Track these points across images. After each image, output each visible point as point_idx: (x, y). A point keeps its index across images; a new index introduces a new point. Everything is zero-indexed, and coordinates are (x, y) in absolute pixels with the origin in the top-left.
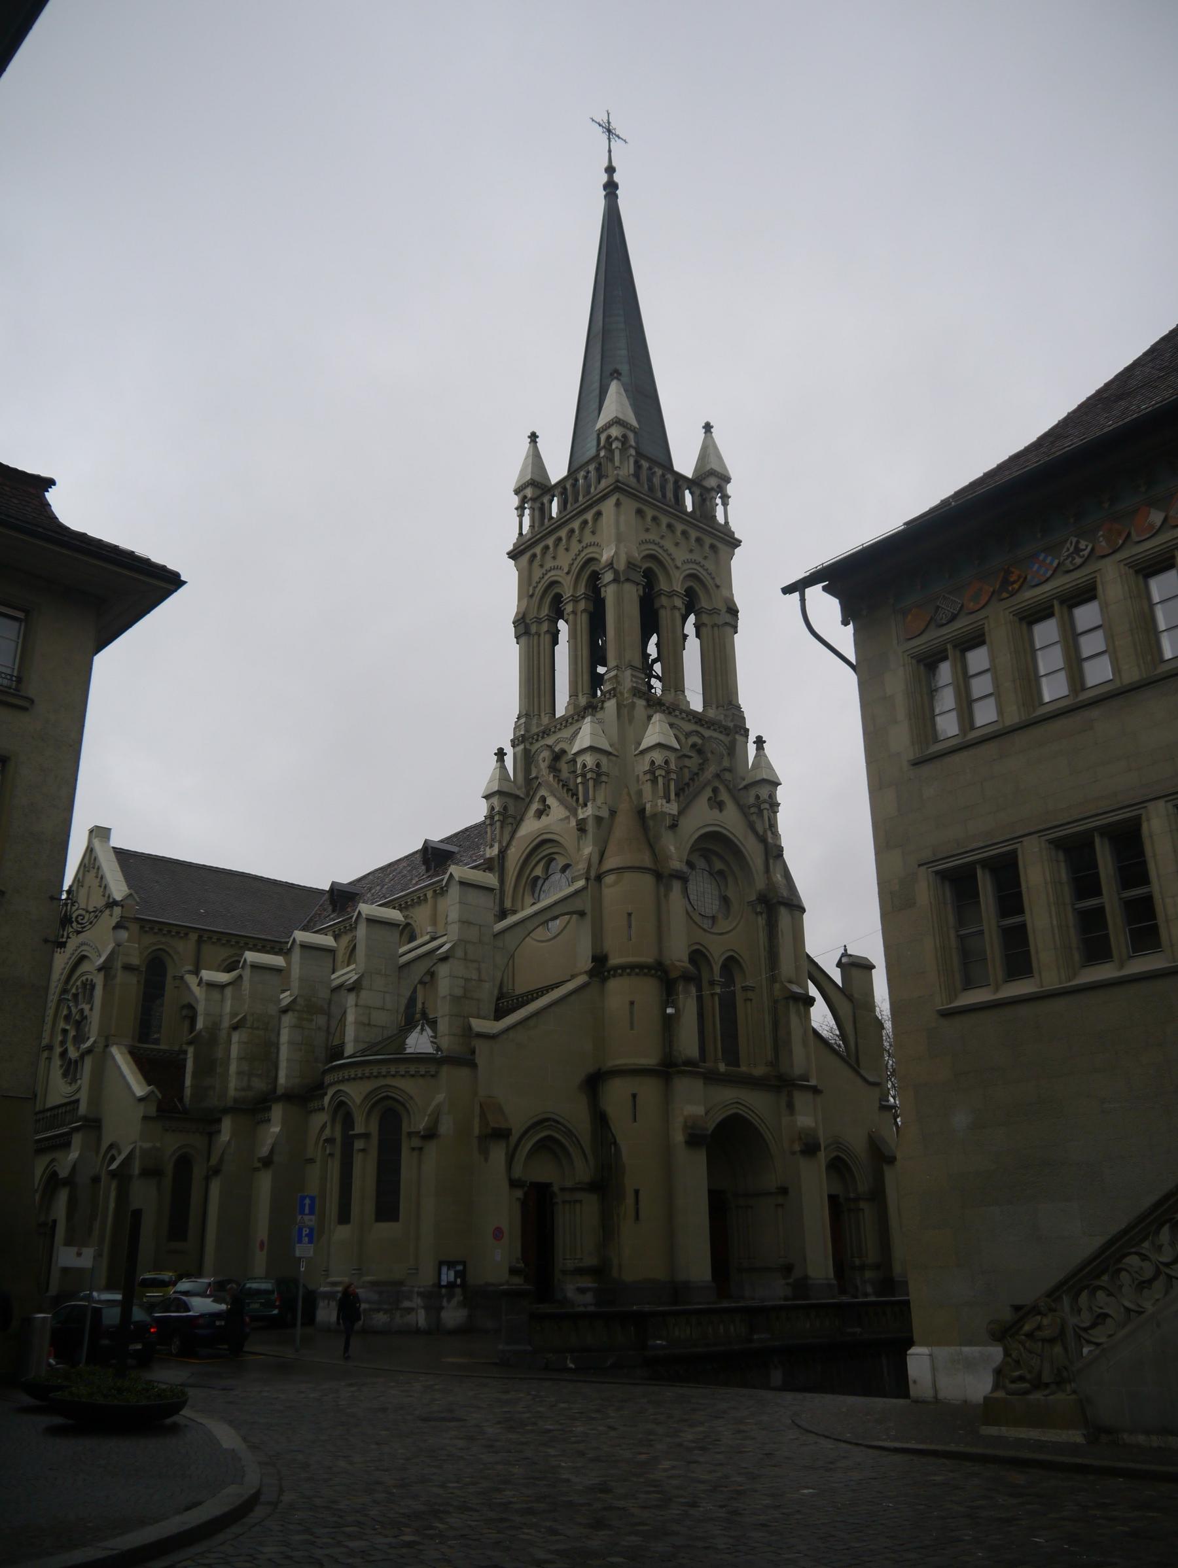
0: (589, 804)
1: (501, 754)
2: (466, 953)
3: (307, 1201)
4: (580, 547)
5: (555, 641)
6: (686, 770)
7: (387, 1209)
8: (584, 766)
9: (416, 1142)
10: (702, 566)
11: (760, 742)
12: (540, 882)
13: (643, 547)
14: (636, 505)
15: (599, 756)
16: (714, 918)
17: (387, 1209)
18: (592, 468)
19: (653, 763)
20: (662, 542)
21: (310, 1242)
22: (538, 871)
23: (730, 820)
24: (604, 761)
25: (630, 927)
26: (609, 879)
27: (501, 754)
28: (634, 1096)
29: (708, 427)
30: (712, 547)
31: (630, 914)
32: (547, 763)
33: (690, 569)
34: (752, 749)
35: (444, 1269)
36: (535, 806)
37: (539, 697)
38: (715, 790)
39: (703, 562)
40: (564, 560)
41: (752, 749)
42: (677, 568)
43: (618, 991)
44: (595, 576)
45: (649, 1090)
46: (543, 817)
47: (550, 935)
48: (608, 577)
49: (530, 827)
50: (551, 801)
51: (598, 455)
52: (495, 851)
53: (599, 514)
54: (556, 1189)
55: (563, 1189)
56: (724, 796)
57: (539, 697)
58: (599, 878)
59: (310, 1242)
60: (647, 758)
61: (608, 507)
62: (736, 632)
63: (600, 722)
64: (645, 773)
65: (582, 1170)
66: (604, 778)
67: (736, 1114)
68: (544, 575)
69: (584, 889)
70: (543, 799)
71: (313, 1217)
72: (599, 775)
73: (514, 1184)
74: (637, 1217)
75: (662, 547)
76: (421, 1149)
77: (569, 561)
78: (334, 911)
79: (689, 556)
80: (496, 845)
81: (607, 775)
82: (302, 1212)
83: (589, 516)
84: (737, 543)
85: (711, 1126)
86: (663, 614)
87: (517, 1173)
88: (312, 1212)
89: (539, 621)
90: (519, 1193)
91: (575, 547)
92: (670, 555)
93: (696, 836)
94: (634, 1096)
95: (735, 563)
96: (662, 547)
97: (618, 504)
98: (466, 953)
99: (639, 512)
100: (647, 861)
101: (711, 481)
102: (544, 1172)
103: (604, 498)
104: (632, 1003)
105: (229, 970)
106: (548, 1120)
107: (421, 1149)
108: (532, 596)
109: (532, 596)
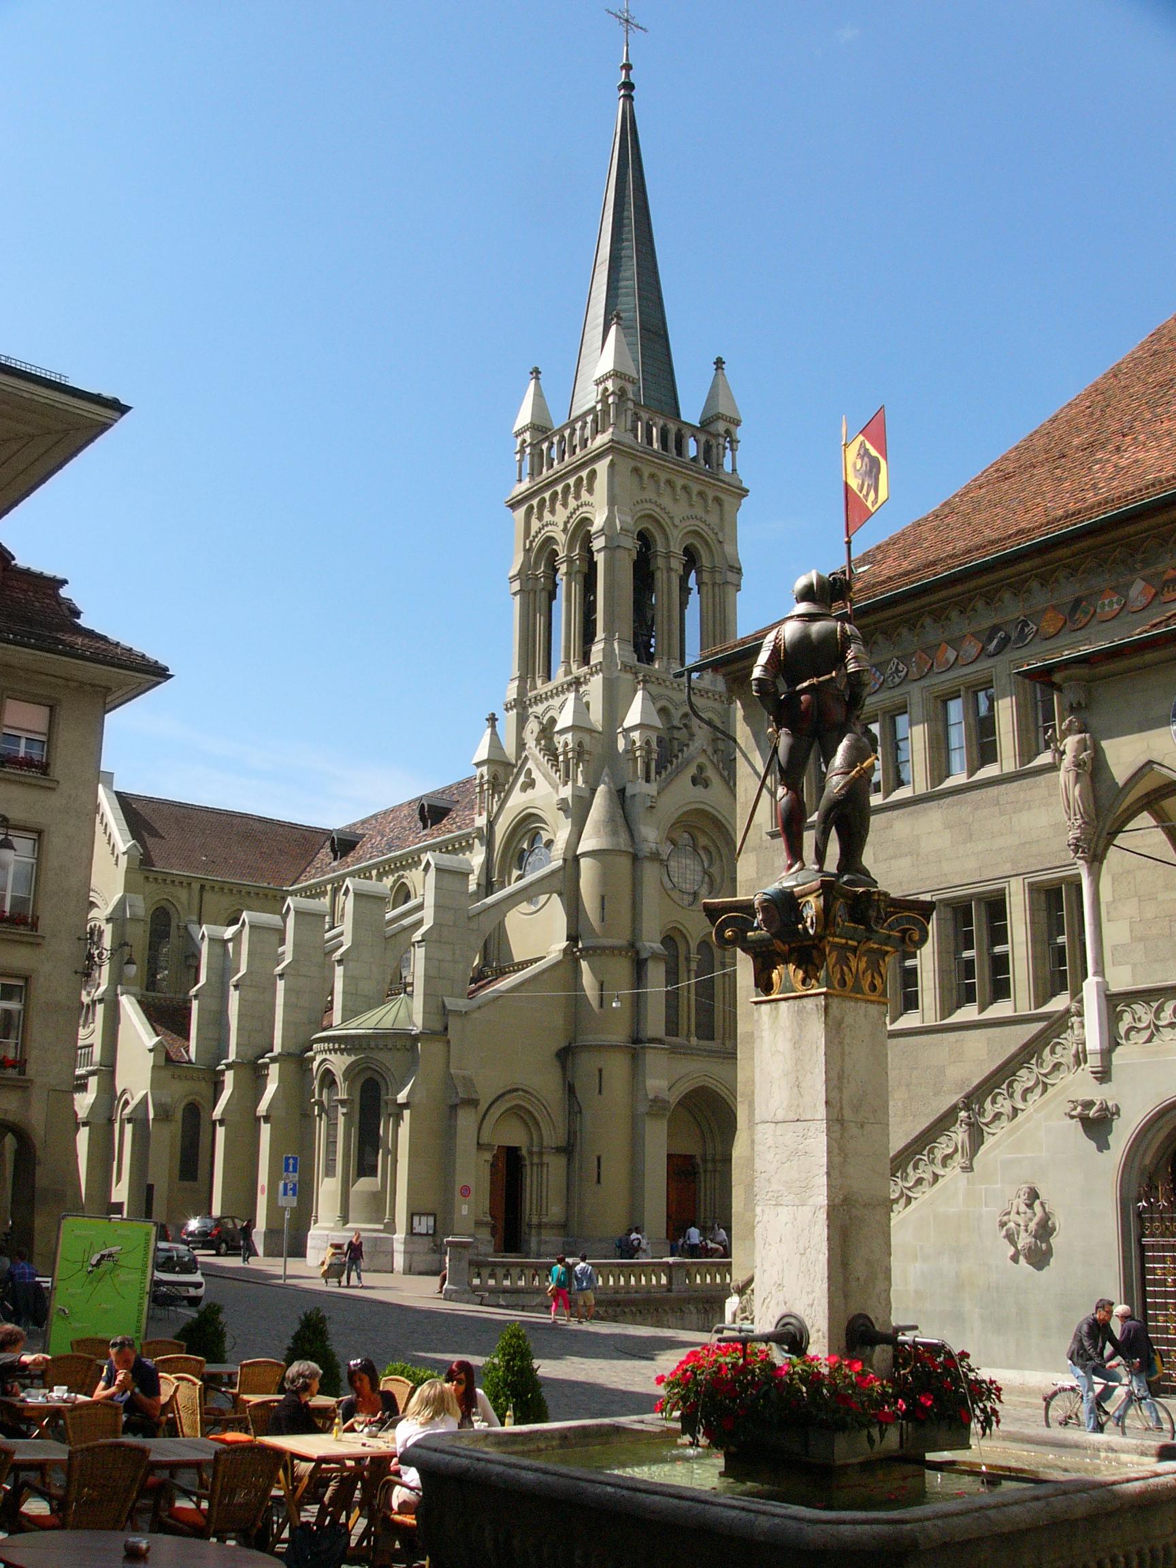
2: (440, 936)
3: (291, 1161)
5: (552, 596)
6: (676, 742)
9: (391, 1109)
12: (526, 854)
14: (633, 464)
15: (580, 734)
18: (589, 419)
21: (294, 1194)
28: (600, 1071)
30: (717, 500)
32: (535, 734)
33: (692, 525)
35: (416, 1219)
36: (522, 779)
38: (701, 768)
40: (561, 514)
44: (588, 538)
46: (529, 791)
47: (533, 908)
48: (599, 543)
49: (518, 800)
50: (536, 774)
51: (595, 407)
52: (481, 821)
54: (524, 1152)
59: (294, 1194)
61: (602, 467)
65: (553, 1135)
70: (529, 772)
71: (297, 1175)
73: (480, 1146)
74: (599, 1181)
75: (659, 506)
77: (565, 519)
78: (335, 859)
80: (485, 814)
81: (590, 753)
82: (287, 1170)
85: (673, 1099)
86: (658, 575)
87: (485, 1139)
88: (295, 1171)
90: (488, 1156)
93: (685, 809)
96: (659, 506)
98: (440, 936)
101: (718, 430)
102: (514, 1136)
103: (599, 457)
106: (516, 1090)
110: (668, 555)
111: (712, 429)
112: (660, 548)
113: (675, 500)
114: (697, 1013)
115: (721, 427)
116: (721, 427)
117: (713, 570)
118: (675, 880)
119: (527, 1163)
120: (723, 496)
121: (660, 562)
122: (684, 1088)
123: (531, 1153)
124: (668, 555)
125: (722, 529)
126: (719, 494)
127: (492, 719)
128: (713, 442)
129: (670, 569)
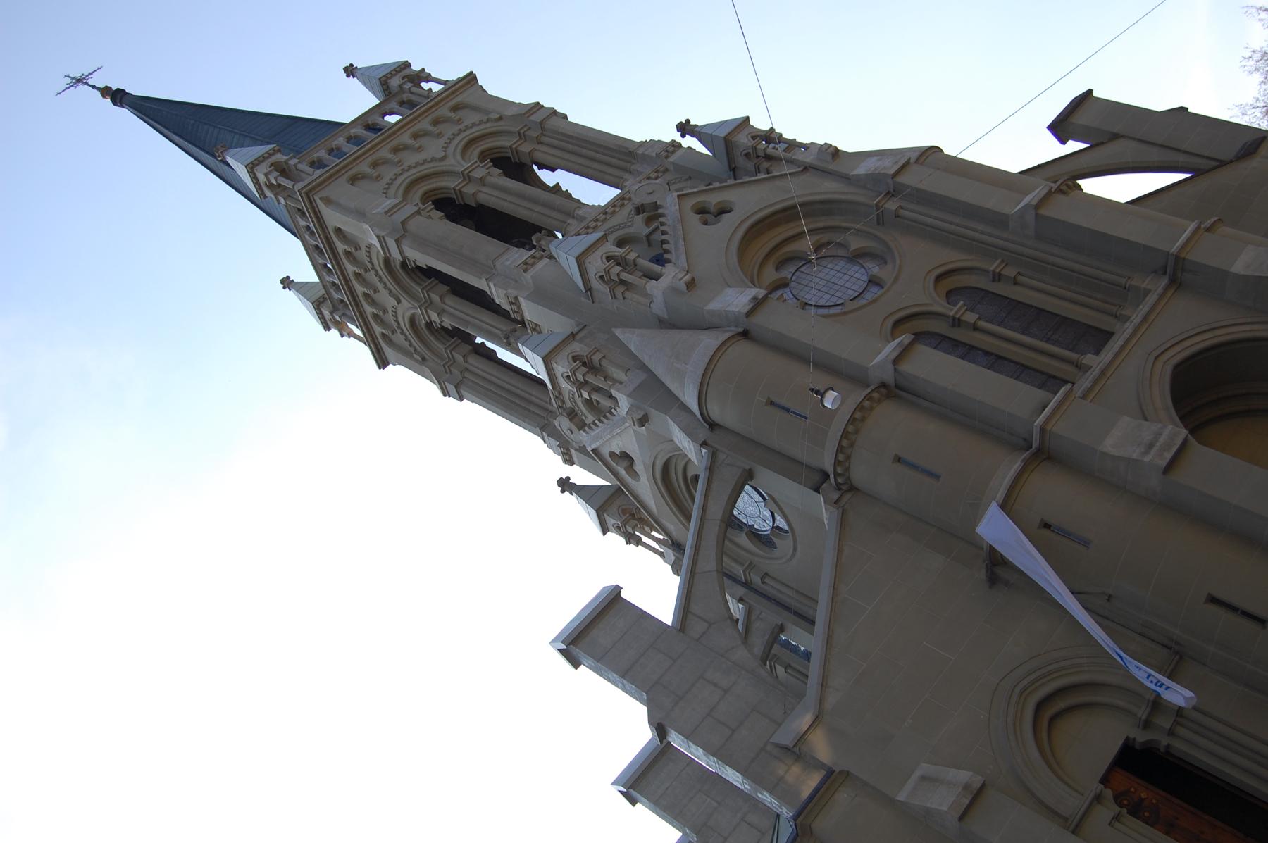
0: (614, 393)
1: (565, 484)
4: (373, 272)
10: (467, 128)
11: (685, 128)
13: (392, 191)
16: (874, 281)
20: (405, 166)
23: (751, 200)
24: (576, 347)
25: (788, 410)
26: (715, 412)
27: (565, 484)
29: (350, 71)
34: (689, 142)
37: (530, 402)
39: (462, 127)
41: (689, 142)
42: (444, 158)
53: (338, 231)
54: (1141, 737)
55: (1147, 725)
56: (713, 200)
57: (530, 402)
58: (713, 426)
60: (596, 284)
62: (565, 117)
64: (614, 296)
66: (596, 358)
67: (1176, 367)
68: (402, 333)
69: (714, 456)
79: (441, 142)
83: (341, 247)
84: (471, 78)
91: (371, 276)
92: (425, 162)
95: (492, 90)
97: (328, 201)
99: (354, 180)
100: (708, 342)
108: (424, 359)
109: (424, 359)
110: (467, 177)
111: (394, 90)
112: (451, 183)
113: (420, 149)
114: (1055, 343)
115: (395, 82)
116: (395, 82)
117: (522, 136)
118: (834, 301)
119: (1165, 741)
120: (459, 99)
121: (469, 190)
122: (1161, 396)
123: (1147, 725)
124: (467, 177)
125: (487, 112)
126: (451, 104)
128: (405, 97)
129: (482, 181)
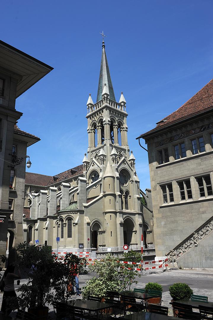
7: (70, 236)
8: (101, 158)
15: (104, 156)
17: (70, 236)
19: (113, 157)
22: (93, 176)
31: (109, 184)
36: (92, 164)
43: (108, 198)
45: (113, 215)
46: (94, 166)
50: (95, 164)
63: (104, 149)
70: (93, 163)
72: (103, 159)
76: (75, 226)
89: (92, 130)
94: (111, 216)
104: (110, 200)
105: (36, 193)
107: (75, 226)
127: (86, 155)
